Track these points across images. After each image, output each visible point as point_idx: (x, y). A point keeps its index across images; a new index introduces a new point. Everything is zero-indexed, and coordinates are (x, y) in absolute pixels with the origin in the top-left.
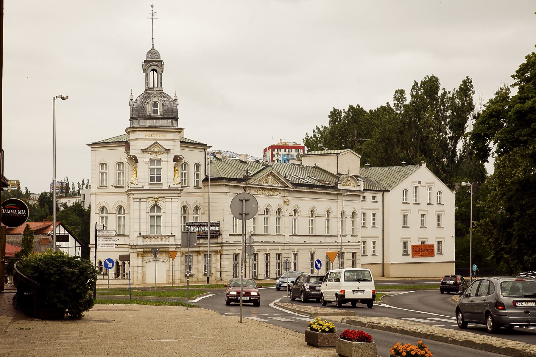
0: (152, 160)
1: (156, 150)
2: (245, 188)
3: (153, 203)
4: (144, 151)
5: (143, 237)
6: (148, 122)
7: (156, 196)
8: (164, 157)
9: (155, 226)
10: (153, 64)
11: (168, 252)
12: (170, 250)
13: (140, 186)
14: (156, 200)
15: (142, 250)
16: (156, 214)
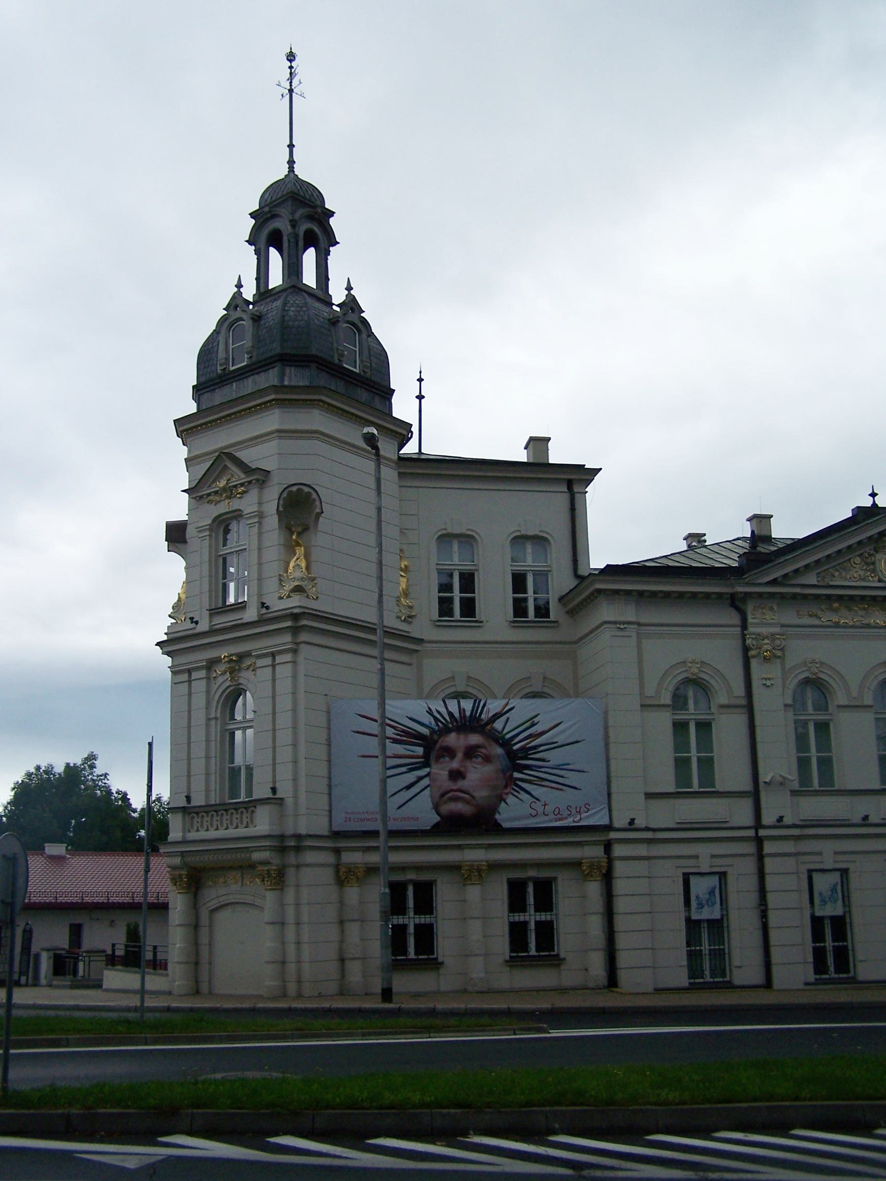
1: (222, 483)
2: (736, 603)
3: (223, 682)
7: (224, 653)
8: (248, 504)
10: (293, 218)
11: (252, 866)
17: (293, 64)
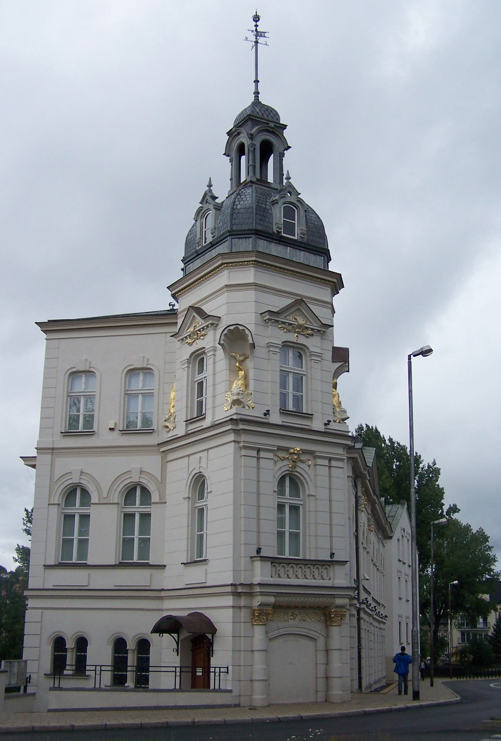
0: (286, 345)
1: (301, 321)
4: (272, 317)
5: (273, 561)
6: (276, 249)
9: (287, 534)
12: (339, 601)
13: (258, 413)
14: (296, 459)
15: (271, 600)
16: (288, 499)
17: (258, 23)
